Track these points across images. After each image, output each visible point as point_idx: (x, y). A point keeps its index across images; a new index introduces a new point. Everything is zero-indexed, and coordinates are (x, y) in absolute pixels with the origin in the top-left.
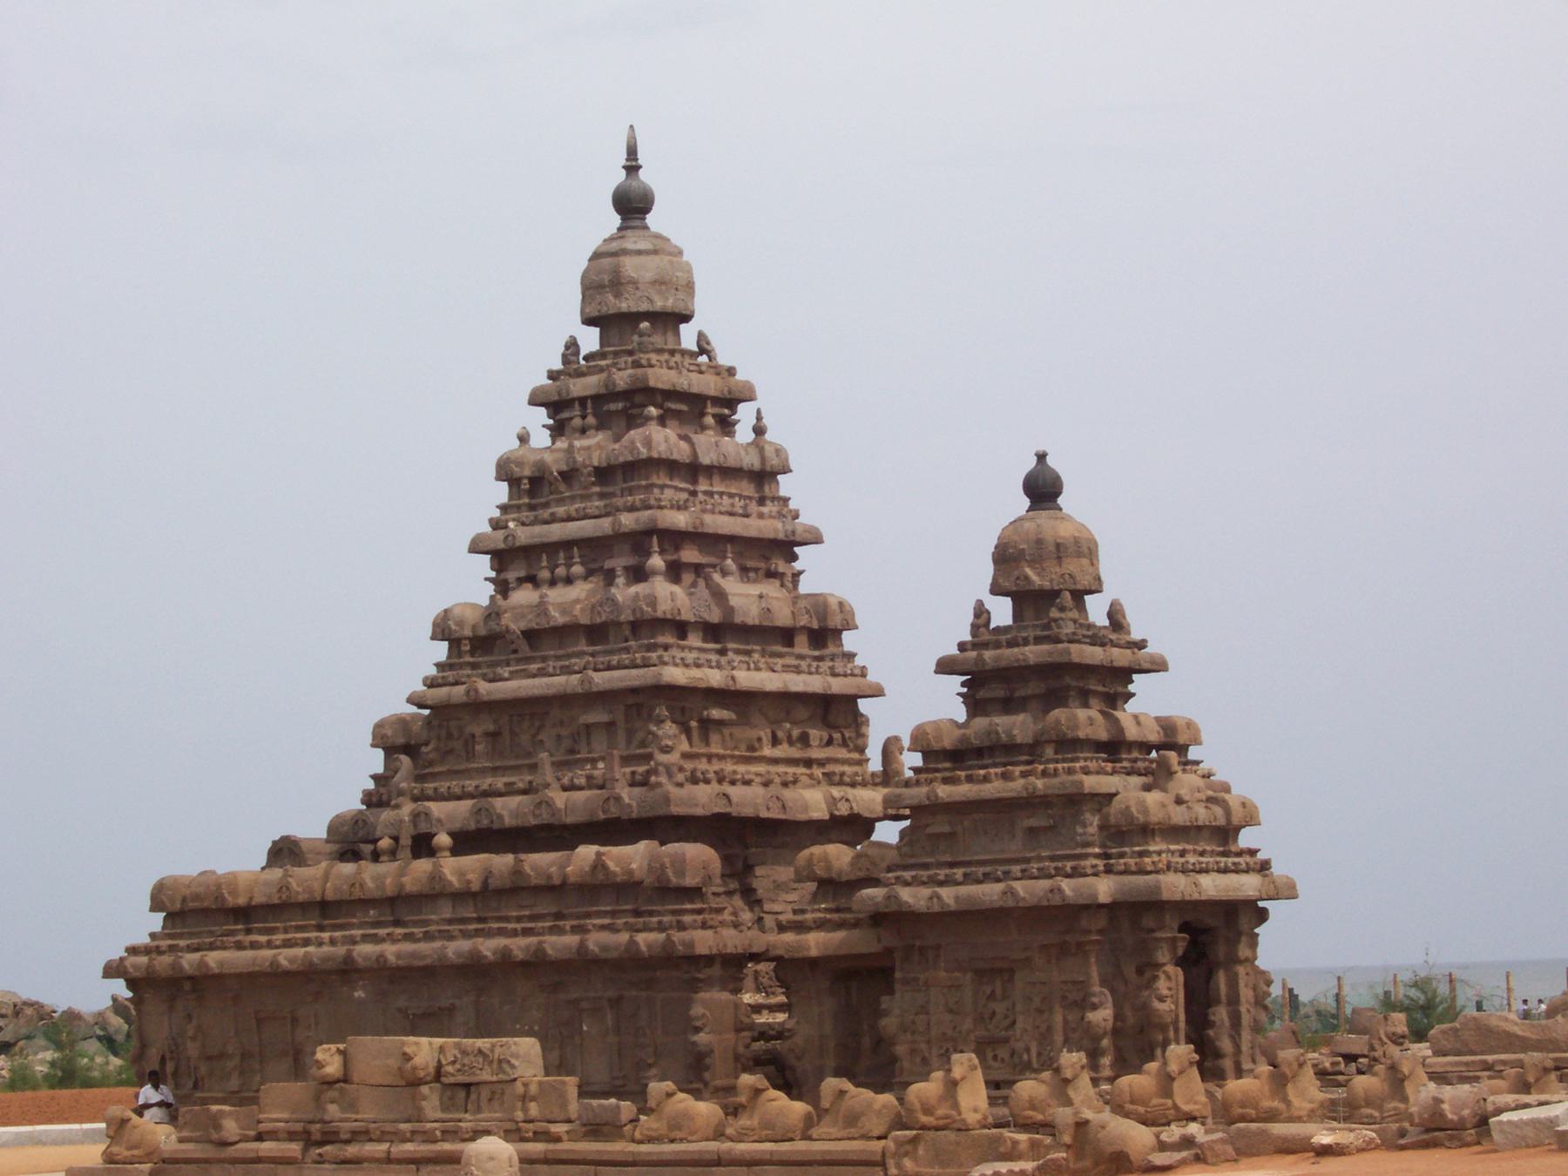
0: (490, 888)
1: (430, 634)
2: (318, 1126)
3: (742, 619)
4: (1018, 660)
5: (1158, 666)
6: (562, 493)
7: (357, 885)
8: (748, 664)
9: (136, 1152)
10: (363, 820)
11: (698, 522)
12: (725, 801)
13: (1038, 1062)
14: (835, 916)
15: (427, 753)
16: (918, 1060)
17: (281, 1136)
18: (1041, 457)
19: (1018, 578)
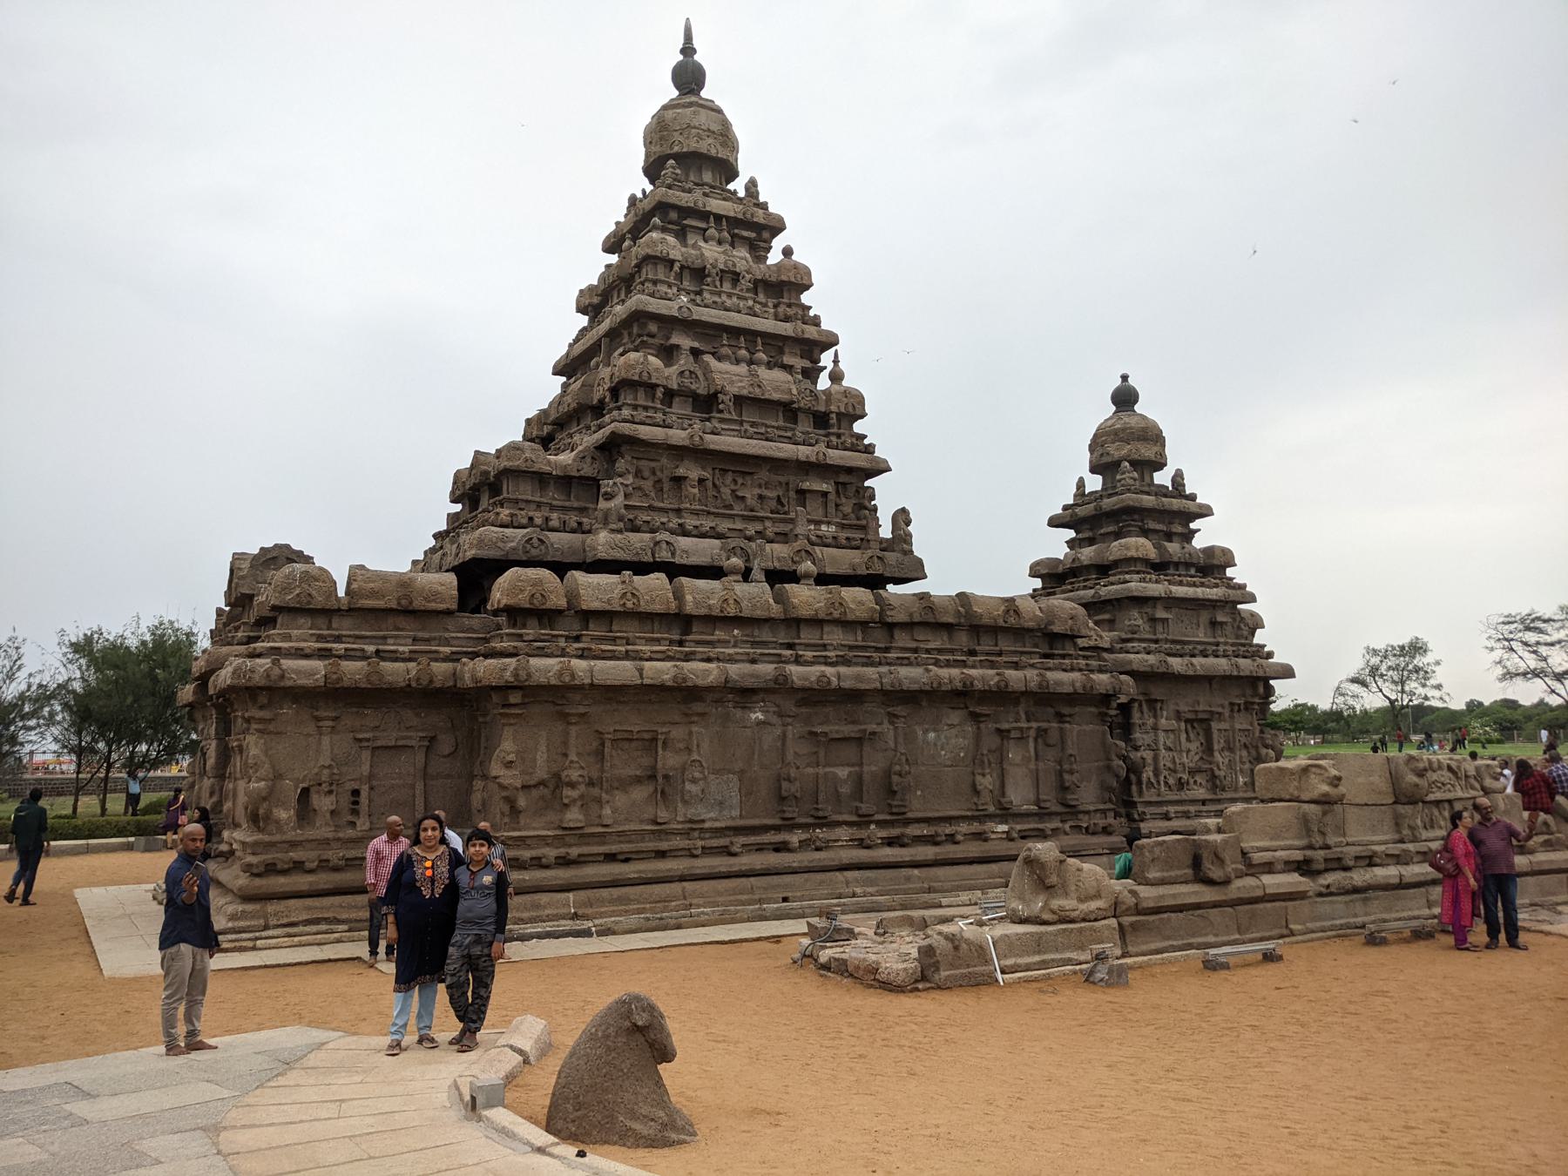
2: (1322, 853)
6: (716, 287)
7: (731, 601)
9: (1094, 905)
10: (540, 540)
17: (1279, 867)
18: (1125, 378)
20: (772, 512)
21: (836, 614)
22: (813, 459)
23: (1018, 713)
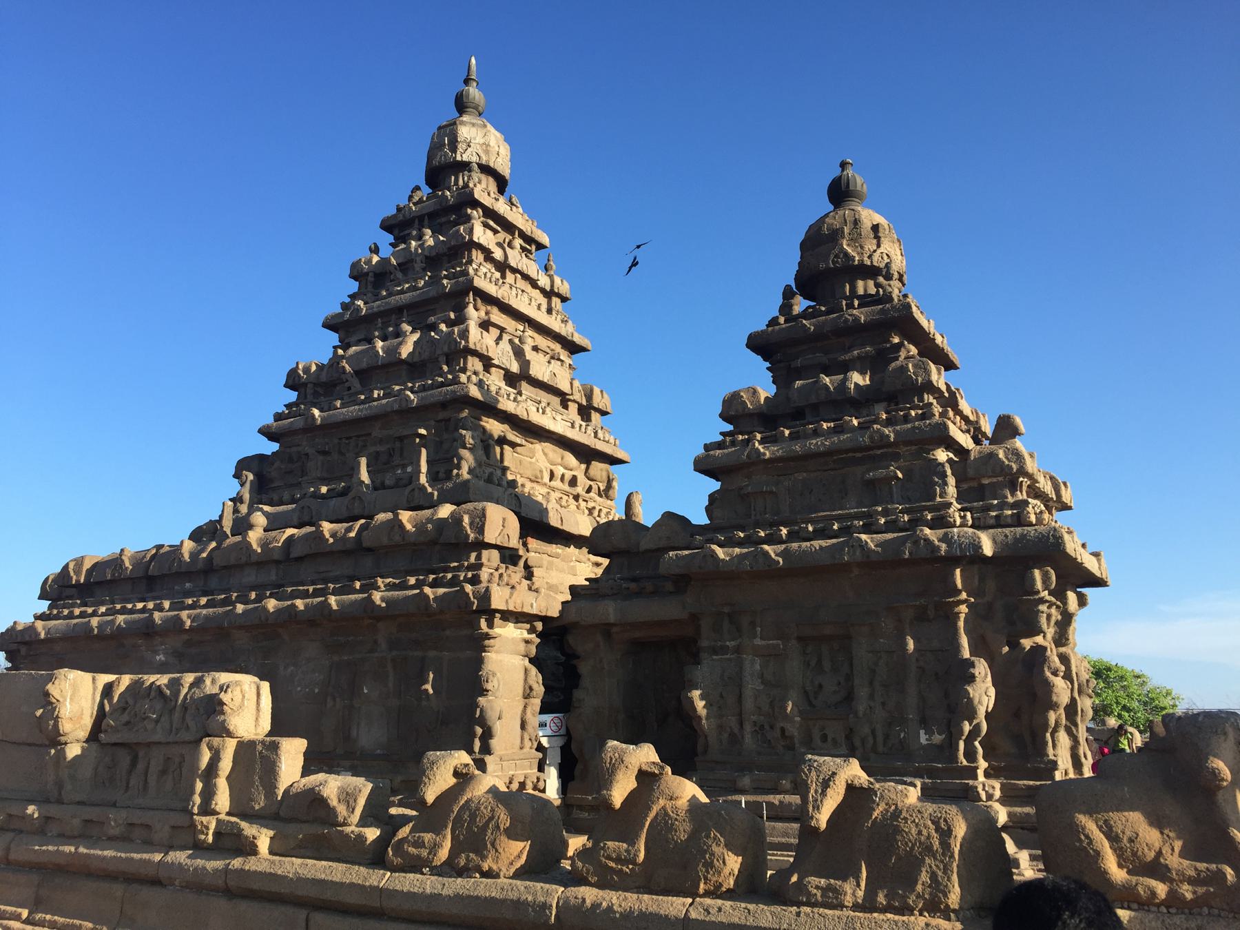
0: (292, 556)
1: (284, 383)
3: (535, 374)
4: (846, 320)
5: (948, 365)
8: (538, 409)
11: (506, 294)
12: (514, 502)
13: (885, 744)
14: (633, 586)
15: (270, 472)
16: (726, 735)
19: (837, 256)
20: (385, 464)
21: (244, 559)
22: (396, 407)
23: (376, 642)
